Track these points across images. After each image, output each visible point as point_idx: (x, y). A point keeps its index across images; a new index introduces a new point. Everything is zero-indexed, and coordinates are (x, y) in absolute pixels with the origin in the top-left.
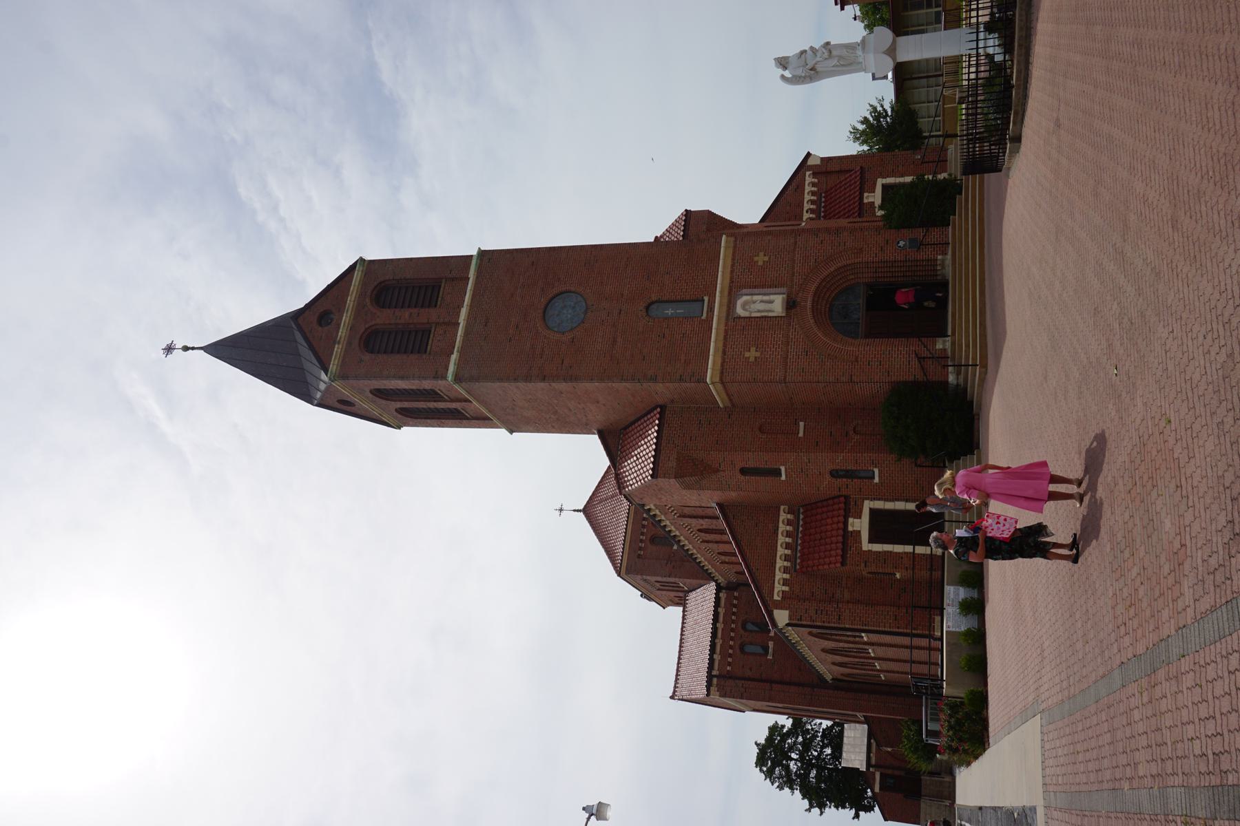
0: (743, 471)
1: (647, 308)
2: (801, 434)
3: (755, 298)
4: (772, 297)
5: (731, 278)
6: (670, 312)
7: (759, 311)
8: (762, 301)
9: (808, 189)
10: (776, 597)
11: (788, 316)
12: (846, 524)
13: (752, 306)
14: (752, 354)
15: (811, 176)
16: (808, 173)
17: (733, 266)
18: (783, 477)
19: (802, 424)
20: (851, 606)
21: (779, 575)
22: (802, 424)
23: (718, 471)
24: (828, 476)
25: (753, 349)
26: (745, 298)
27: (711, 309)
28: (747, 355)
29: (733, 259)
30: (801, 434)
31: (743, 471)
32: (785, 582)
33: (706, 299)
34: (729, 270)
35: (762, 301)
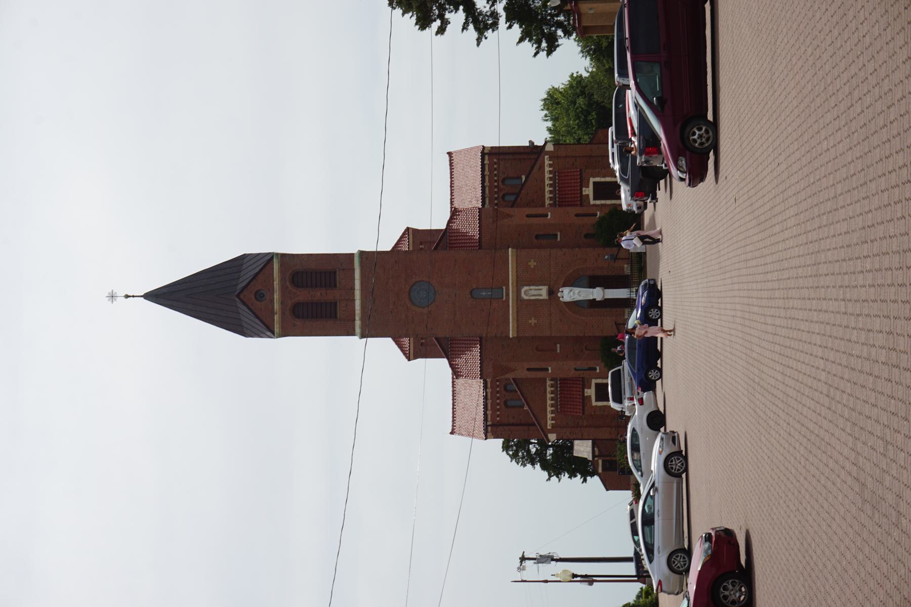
0: (528, 369)
1: (471, 292)
2: (558, 351)
3: (531, 287)
4: (540, 287)
5: (517, 275)
6: (484, 293)
7: (534, 295)
8: (535, 289)
9: (547, 169)
10: (549, 427)
11: (550, 298)
12: (583, 392)
13: (530, 292)
14: (533, 321)
15: (548, 159)
16: (546, 157)
17: (517, 267)
18: (550, 371)
19: (558, 345)
20: (587, 429)
21: (549, 416)
22: (558, 345)
23: (515, 370)
24: (573, 371)
25: (533, 319)
26: (526, 288)
27: (508, 295)
28: (530, 322)
29: (517, 264)
30: (558, 351)
31: (528, 369)
32: (553, 419)
33: (504, 288)
34: (515, 270)
35: (535, 289)
